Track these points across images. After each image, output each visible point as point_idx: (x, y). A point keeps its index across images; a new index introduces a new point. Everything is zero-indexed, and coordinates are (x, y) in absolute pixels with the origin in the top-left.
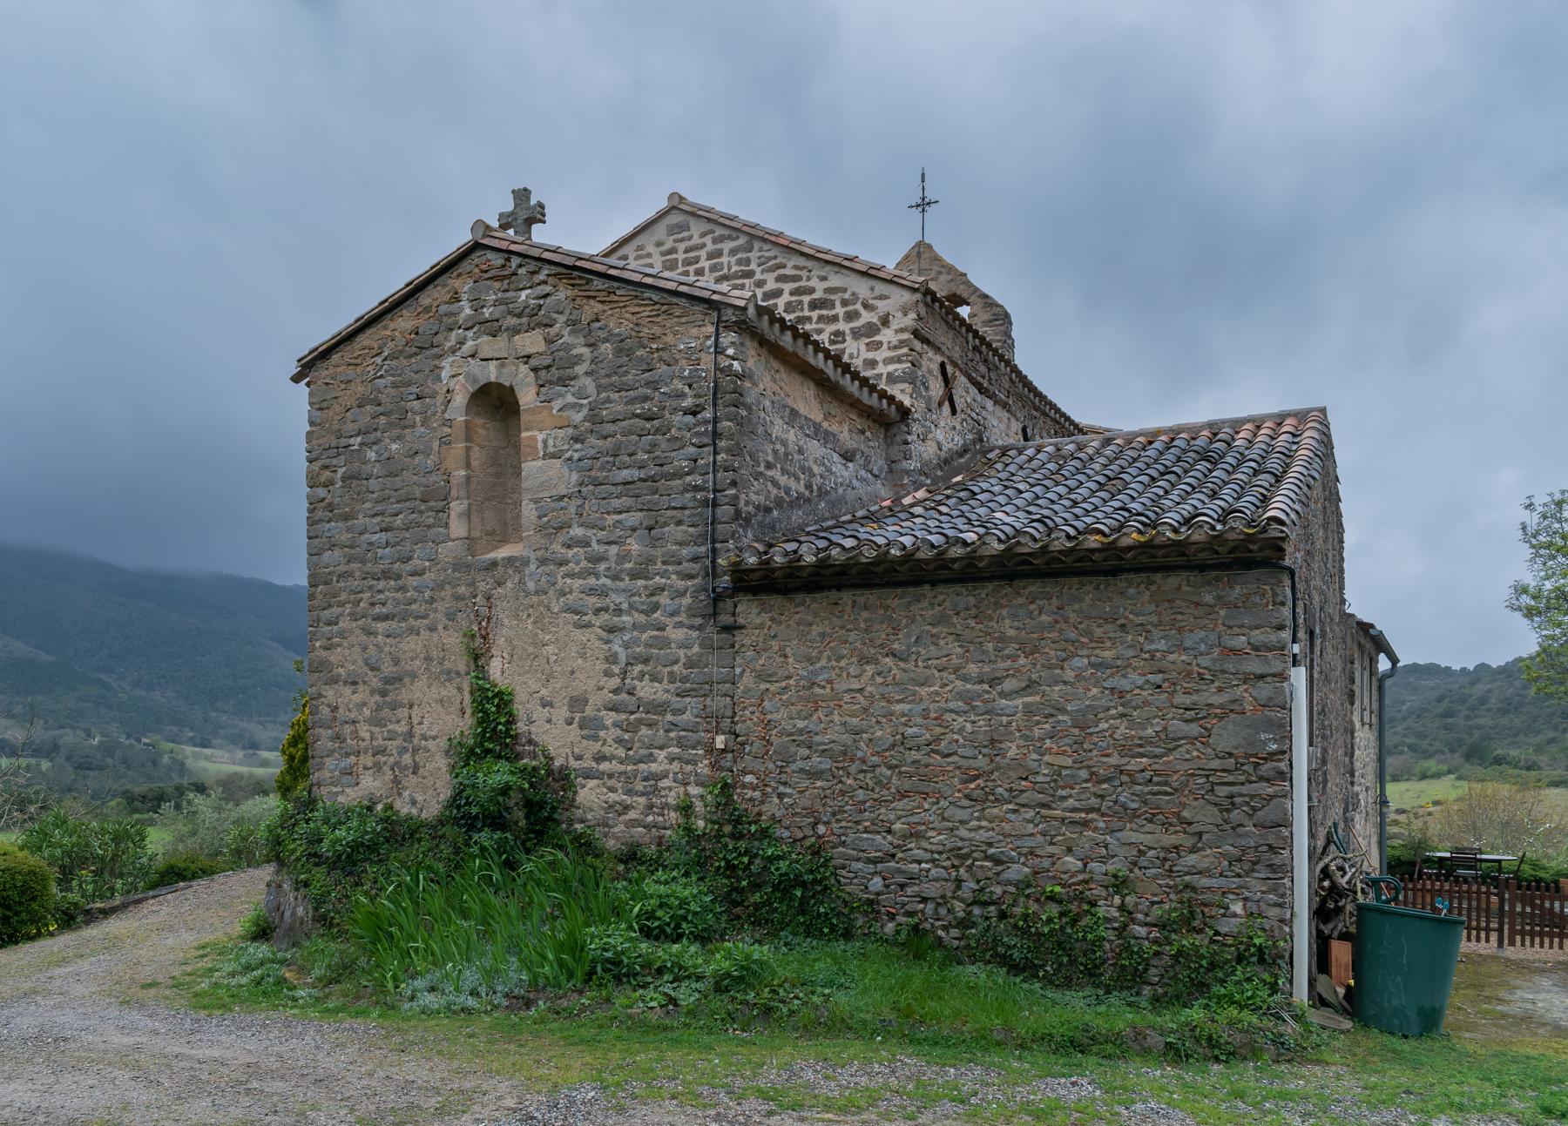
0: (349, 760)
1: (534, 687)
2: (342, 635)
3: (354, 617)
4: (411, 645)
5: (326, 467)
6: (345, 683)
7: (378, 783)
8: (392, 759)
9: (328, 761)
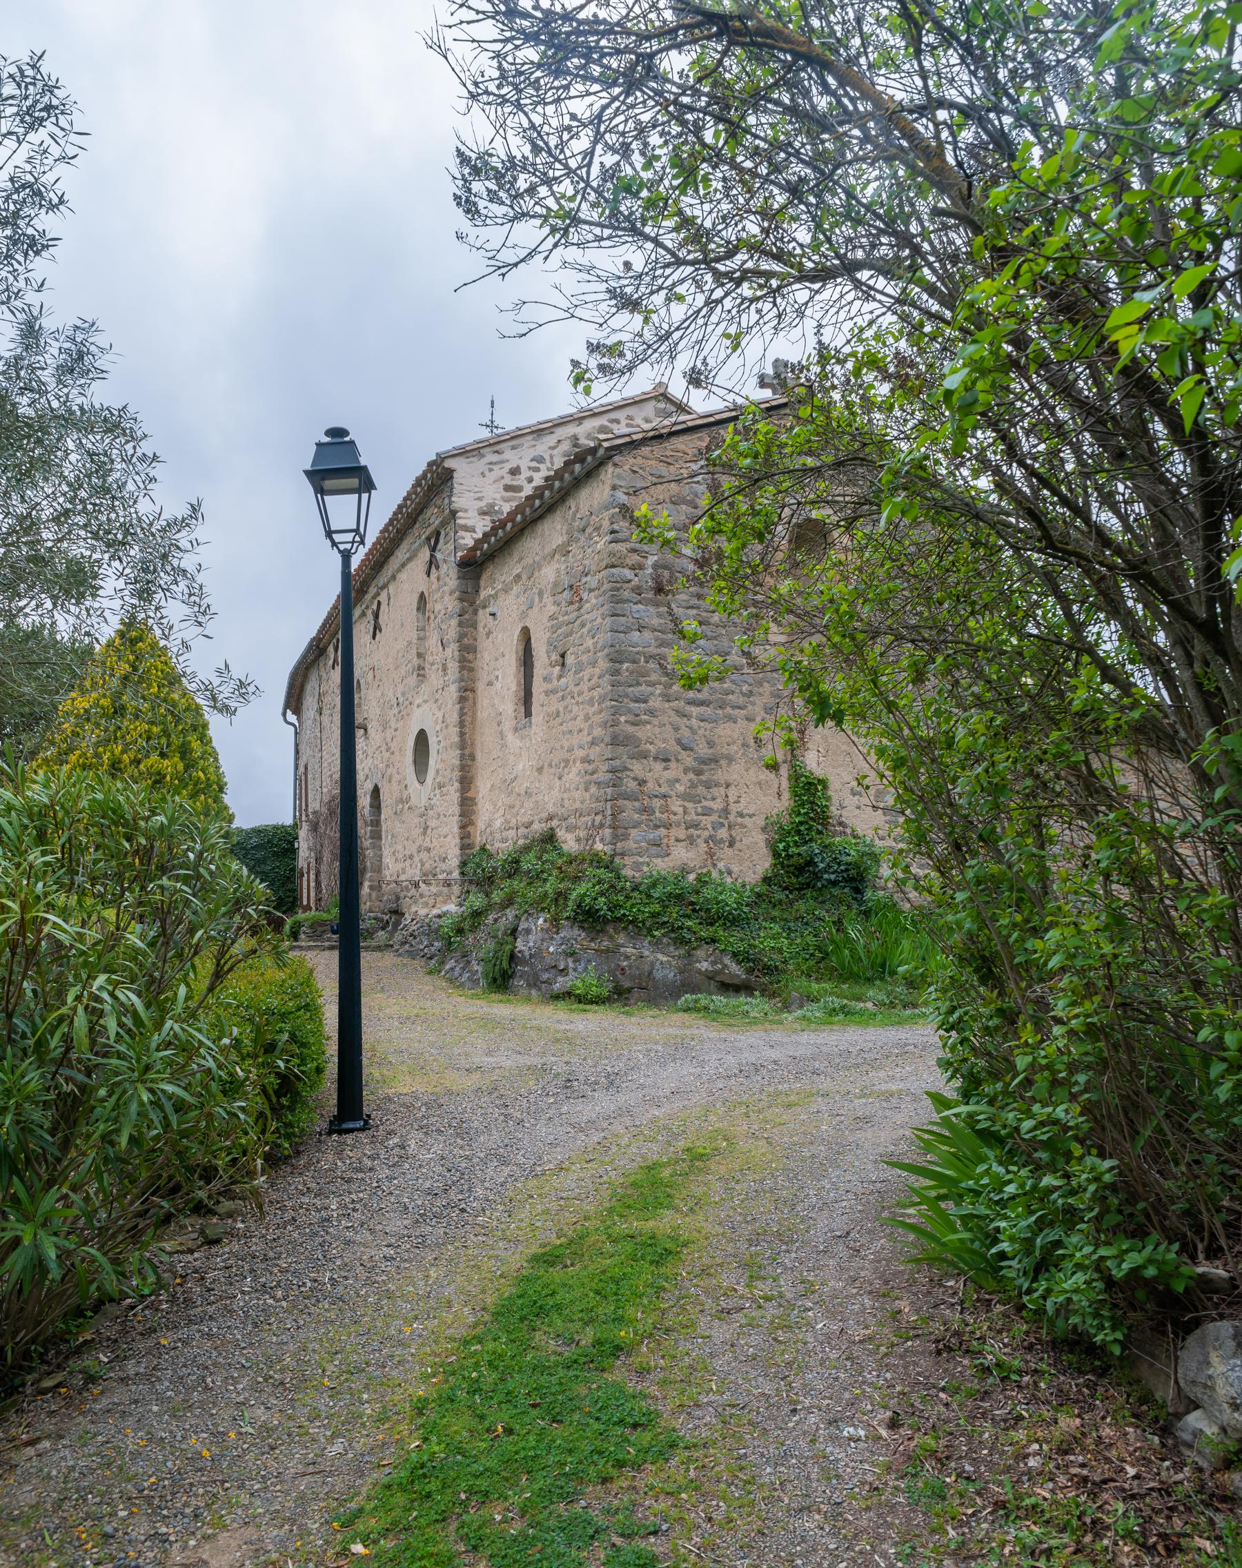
0: (657, 833)
1: (846, 779)
2: (651, 713)
3: (667, 698)
4: (725, 731)
5: (634, 551)
6: (656, 759)
7: (691, 855)
8: (706, 834)
9: (634, 833)
